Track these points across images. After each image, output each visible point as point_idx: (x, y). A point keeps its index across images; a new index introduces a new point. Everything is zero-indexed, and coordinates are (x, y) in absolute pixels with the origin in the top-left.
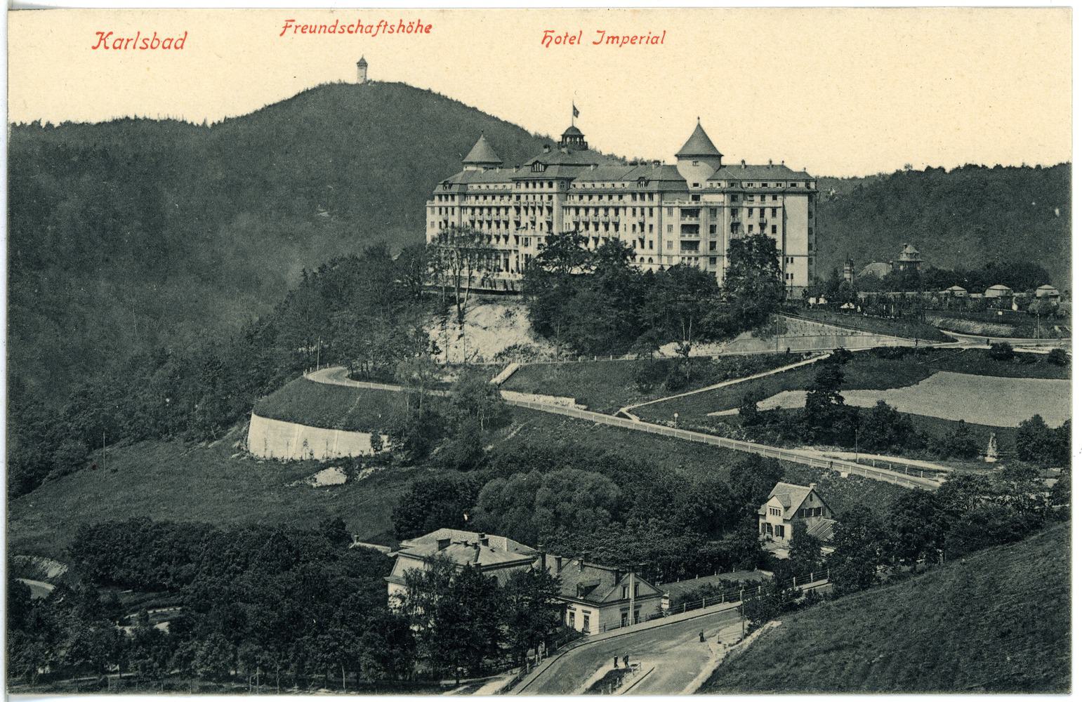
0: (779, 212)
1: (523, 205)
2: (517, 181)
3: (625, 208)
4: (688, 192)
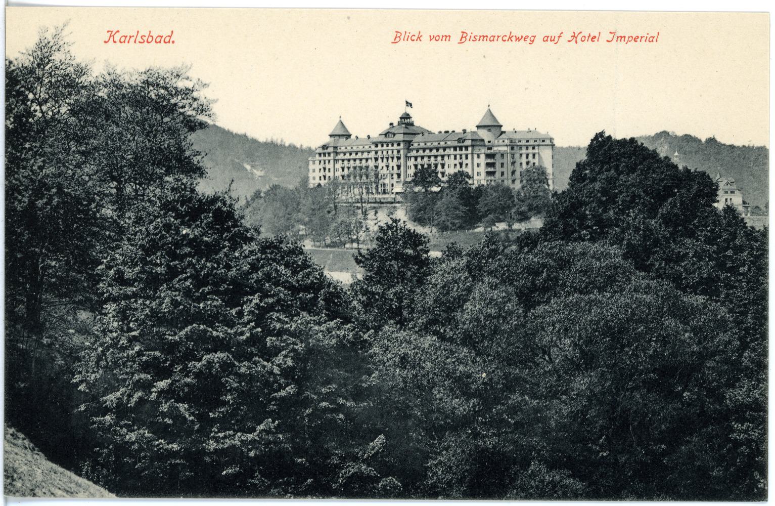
0: (537, 156)
1: (380, 157)
4: (485, 145)
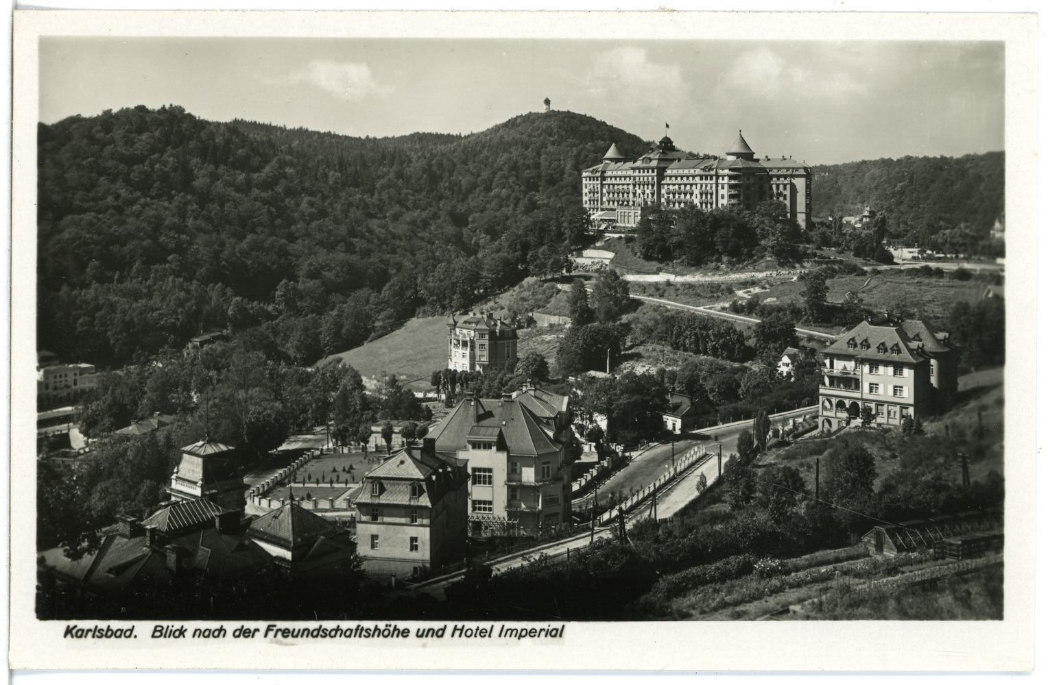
2: (634, 169)
3: (696, 184)
